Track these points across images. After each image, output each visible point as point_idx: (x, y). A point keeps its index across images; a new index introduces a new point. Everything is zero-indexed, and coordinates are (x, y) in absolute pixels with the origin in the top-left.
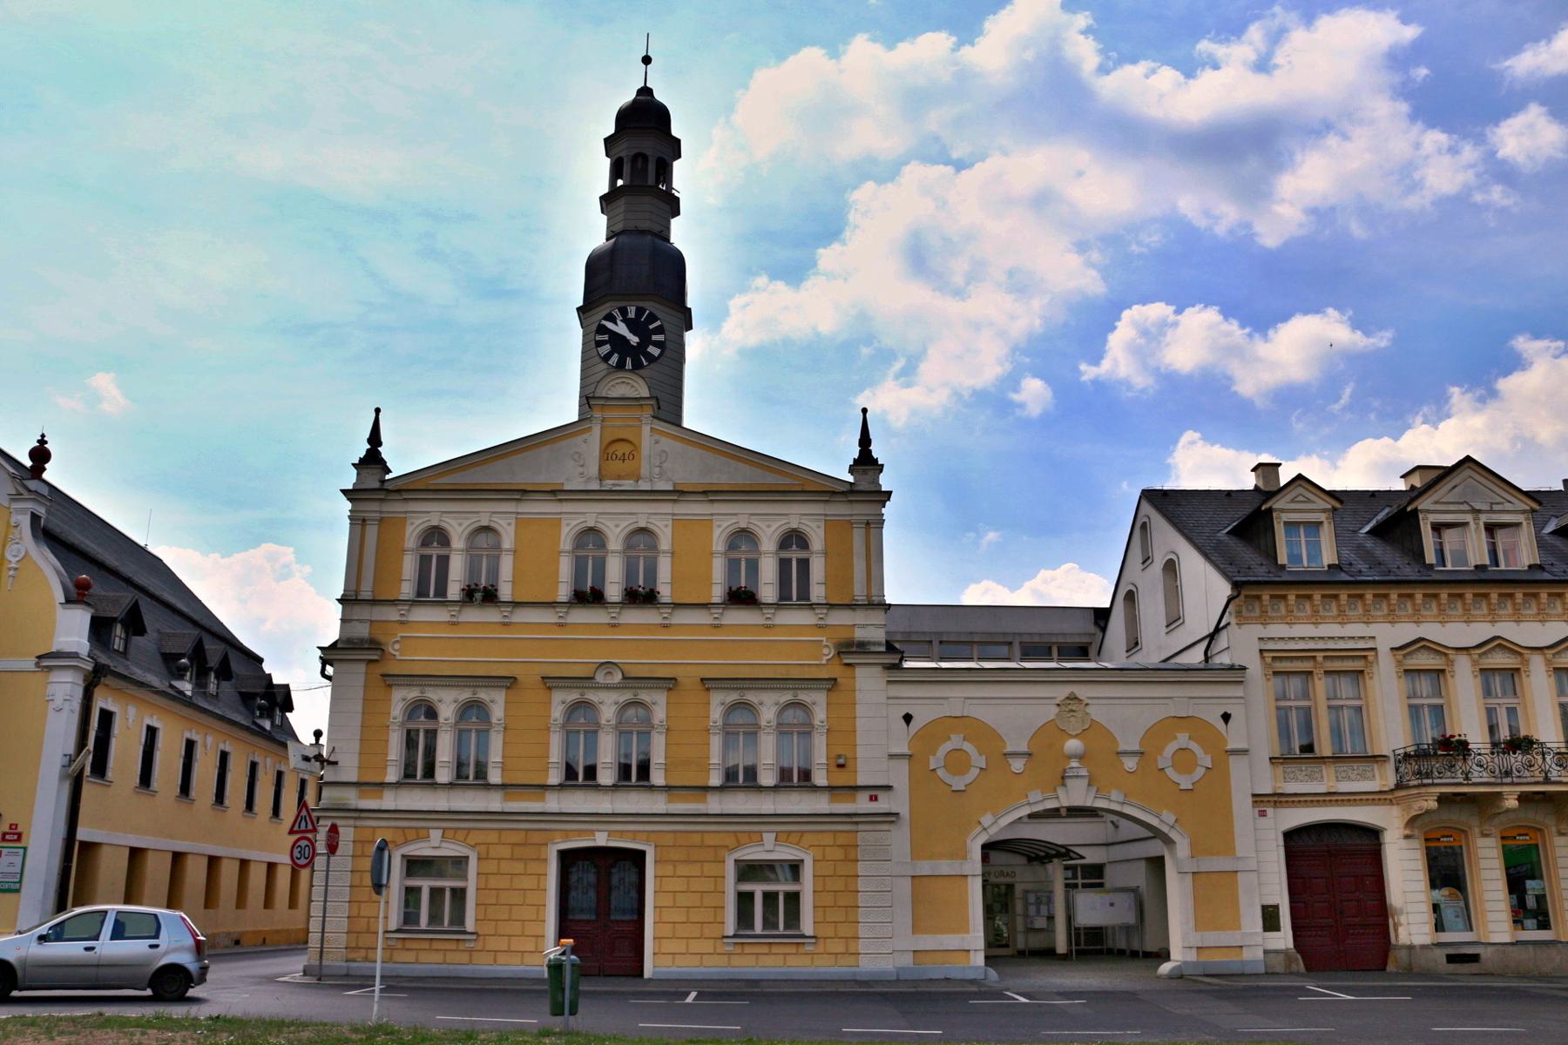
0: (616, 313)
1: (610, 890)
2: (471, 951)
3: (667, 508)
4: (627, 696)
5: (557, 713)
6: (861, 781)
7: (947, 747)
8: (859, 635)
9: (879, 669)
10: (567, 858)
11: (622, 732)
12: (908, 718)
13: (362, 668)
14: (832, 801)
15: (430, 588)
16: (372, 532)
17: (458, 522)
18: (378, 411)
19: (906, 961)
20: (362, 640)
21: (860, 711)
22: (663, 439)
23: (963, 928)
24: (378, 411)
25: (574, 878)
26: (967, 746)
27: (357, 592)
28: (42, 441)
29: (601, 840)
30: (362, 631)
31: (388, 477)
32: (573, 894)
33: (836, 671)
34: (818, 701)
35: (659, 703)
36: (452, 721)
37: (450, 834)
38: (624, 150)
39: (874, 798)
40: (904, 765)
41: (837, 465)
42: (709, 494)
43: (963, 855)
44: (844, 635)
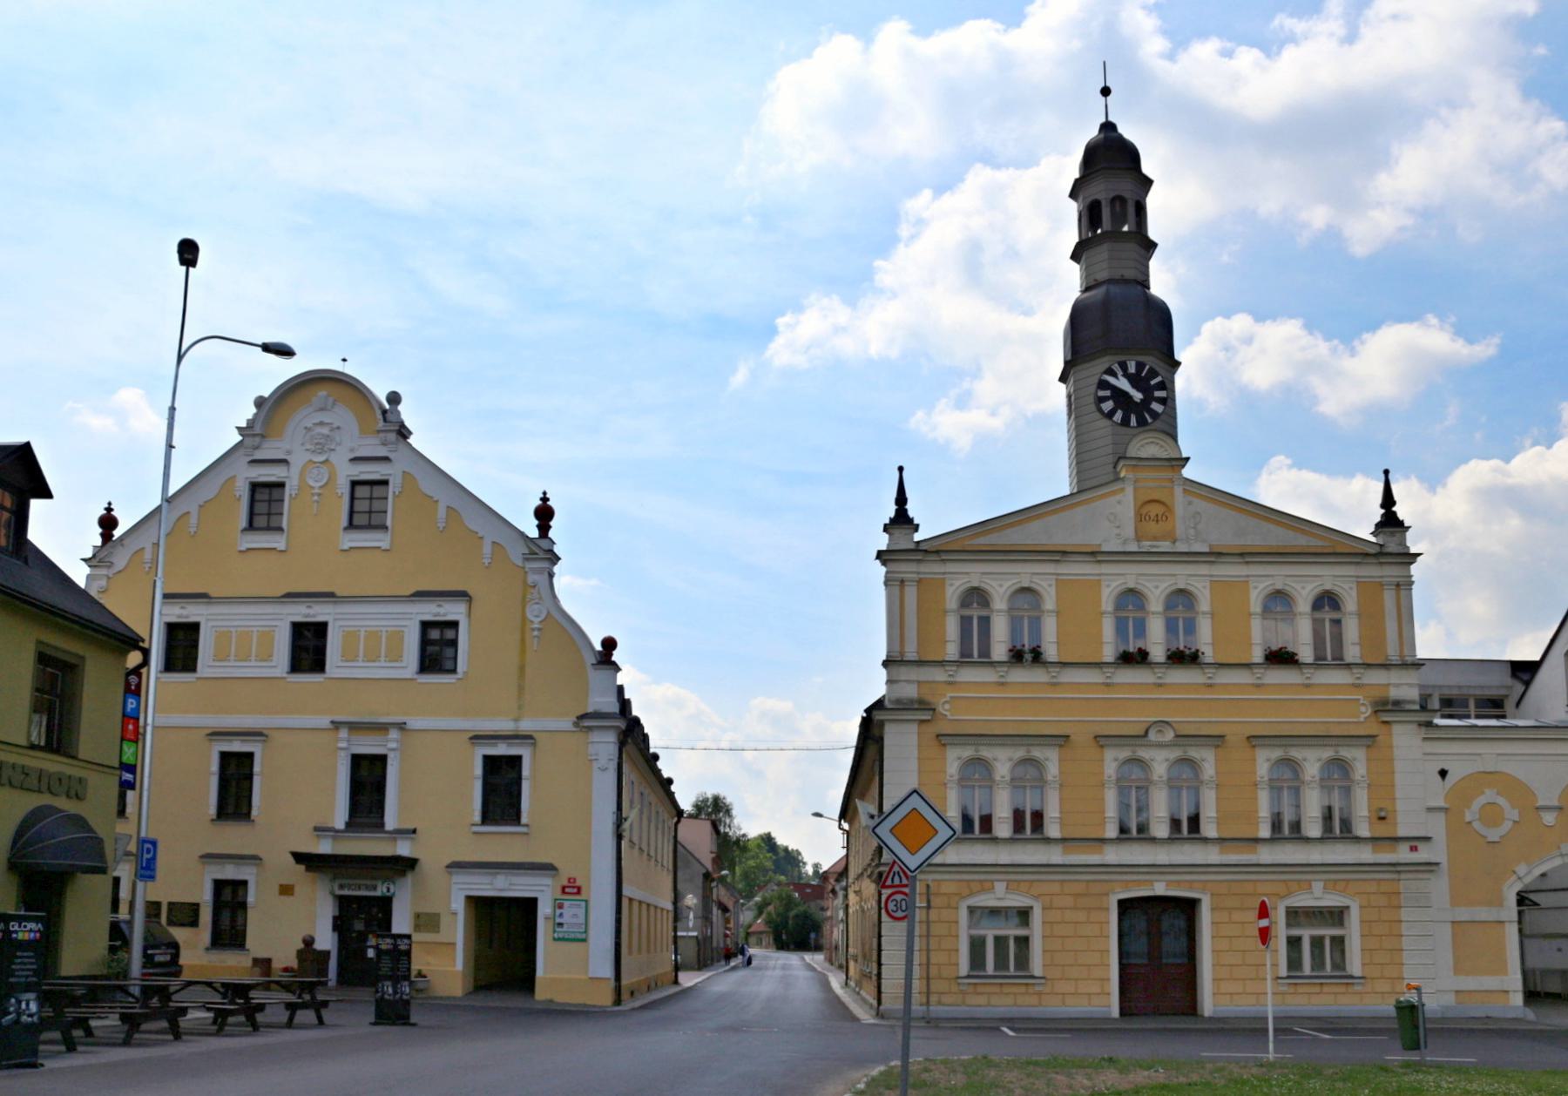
0: (1116, 368)
2: (1040, 994)
3: (1204, 569)
4: (1175, 753)
6: (1401, 833)
7: (1482, 800)
8: (1394, 694)
9: (1414, 726)
11: (1173, 785)
12: (1443, 773)
13: (914, 727)
14: (1374, 851)
15: (974, 651)
16: (911, 593)
17: (1000, 583)
18: (901, 469)
19: (1450, 1000)
20: (911, 701)
22: (1196, 501)
23: (1502, 970)
24: (901, 469)
26: (1501, 801)
27: (902, 653)
28: (545, 499)
29: (1160, 889)
30: (910, 692)
31: (918, 537)
33: (1373, 729)
34: (1358, 758)
35: (1208, 759)
39: (1414, 849)
40: (1441, 816)
41: (1363, 525)
42: (1245, 556)
43: (1499, 903)
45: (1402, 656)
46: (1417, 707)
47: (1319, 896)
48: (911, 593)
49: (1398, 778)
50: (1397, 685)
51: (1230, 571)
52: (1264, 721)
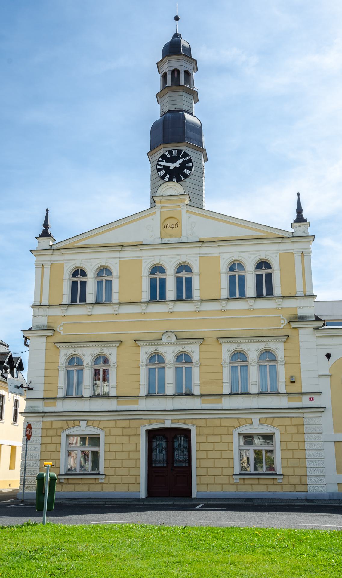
1: (173, 450)
2: (102, 484)
3: (196, 251)
5: (144, 358)
9: (312, 330)
10: (152, 434)
12: (328, 356)
16: (47, 270)
18: (47, 210)
21: (302, 352)
25: (155, 444)
29: (168, 424)
32: (154, 453)
33: (289, 332)
36: (90, 365)
37: (90, 423)
38: (167, 68)
39: (311, 399)
44: (292, 313)
45: (305, 291)
46: (314, 319)
47: (256, 427)
48: (47, 270)
50: (302, 308)
51: (208, 250)
52: (224, 329)
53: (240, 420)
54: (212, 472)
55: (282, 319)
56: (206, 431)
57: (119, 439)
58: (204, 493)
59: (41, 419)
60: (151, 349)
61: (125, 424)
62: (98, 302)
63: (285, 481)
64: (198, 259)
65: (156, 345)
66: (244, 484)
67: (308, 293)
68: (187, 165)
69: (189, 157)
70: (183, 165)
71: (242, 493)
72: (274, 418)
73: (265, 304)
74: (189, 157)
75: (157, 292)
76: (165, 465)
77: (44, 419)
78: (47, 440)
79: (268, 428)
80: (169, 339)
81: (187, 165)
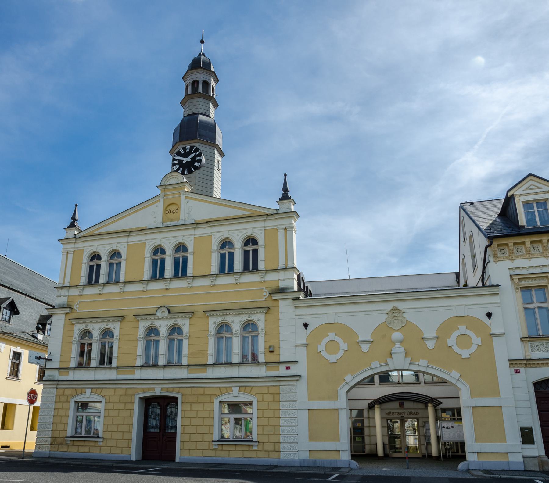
2: (100, 446)
12: (306, 325)
21: (281, 323)
49: (281, 330)
53: (221, 389)
54: (194, 438)
55: (265, 291)
56: (191, 399)
57: (117, 406)
58: (186, 457)
59: (55, 386)
60: (148, 323)
61: (121, 392)
62: (109, 282)
63: (260, 448)
64: (193, 239)
65: (152, 319)
66: (222, 450)
67: (289, 266)
68: (198, 158)
69: (200, 152)
70: (194, 159)
71: (220, 458)
72: (252, 387)
73: (251, 278)
74: (200, 152)
75: (157, 272)
76: (158, 431)
77: (59, 386)
78: (60, 405)
79: (247, 397)
80: (164, 314)
81: (198, 158)
